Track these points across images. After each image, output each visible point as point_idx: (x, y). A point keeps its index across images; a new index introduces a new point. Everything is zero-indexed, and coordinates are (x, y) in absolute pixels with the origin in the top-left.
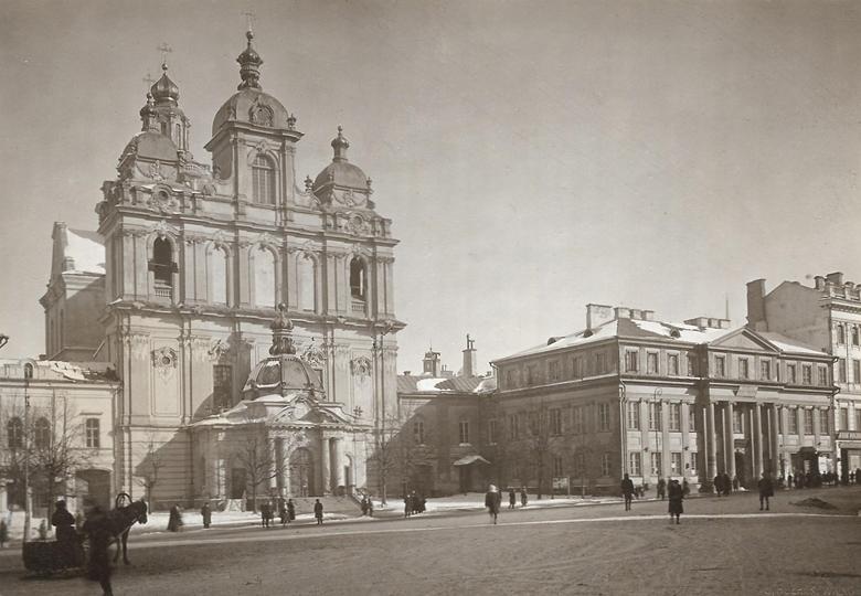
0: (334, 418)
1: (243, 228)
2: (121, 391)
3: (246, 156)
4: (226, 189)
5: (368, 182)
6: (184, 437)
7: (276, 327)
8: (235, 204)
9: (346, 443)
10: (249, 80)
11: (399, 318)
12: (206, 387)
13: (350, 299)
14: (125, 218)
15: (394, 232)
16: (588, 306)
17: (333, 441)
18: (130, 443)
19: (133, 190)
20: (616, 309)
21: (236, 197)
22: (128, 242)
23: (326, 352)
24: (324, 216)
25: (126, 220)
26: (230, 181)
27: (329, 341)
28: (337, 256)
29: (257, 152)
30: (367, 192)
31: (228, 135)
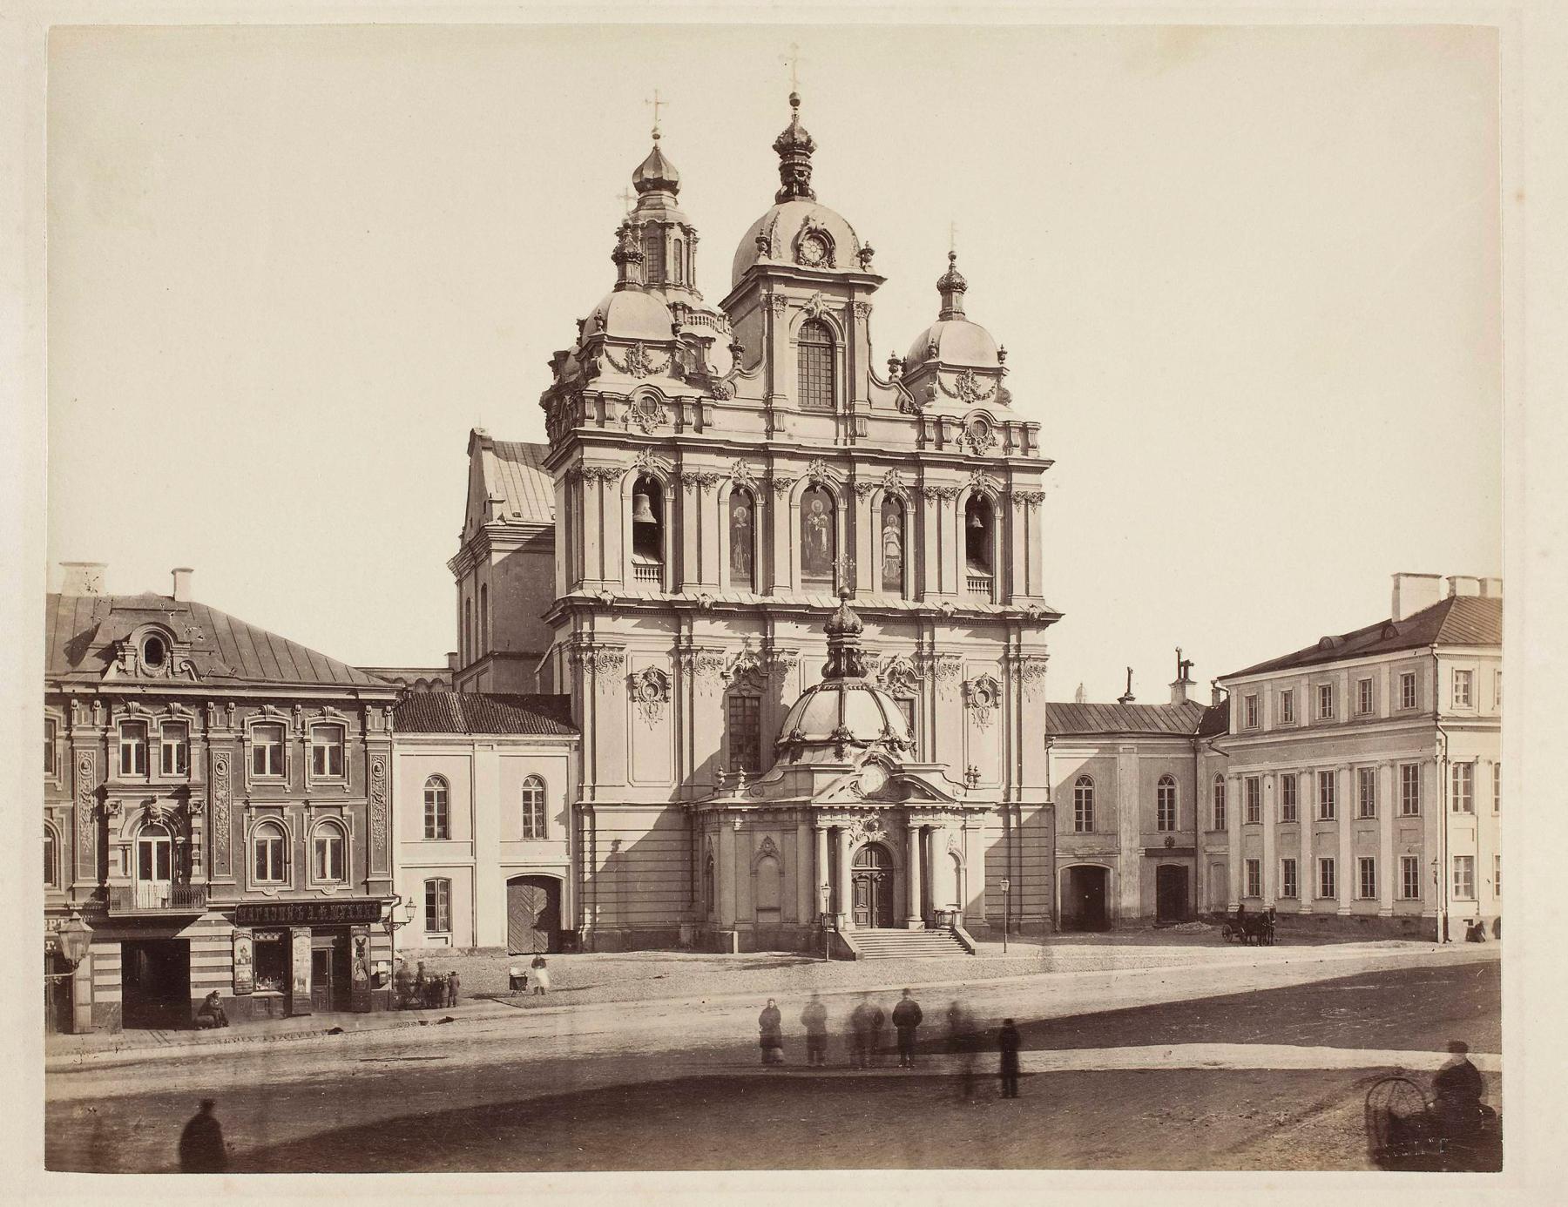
0: (929, 792)
1: (782, 455)
2: (580, 747)
3: (787, 328)
4: (752, 388)
5: (1001, 355)
6: (679, 819)
7: (836, 632)
8: (769, 413)
9: (947, 831)
10: (794, 184)
11: (1052, 604)
12: (711, 734)
13: (967, 570)
14: (586, 449)
15: (1045, 445)
16: (1397, 576)
17: (925, 831)
18: (593, 831)
19: (600, 399)
20: (1452, 580)
21: (768, 399)
22: (591, 487)
23: (921, 669)
24: (920, 423)
25: (589, 452)
26: (760, 372)
27: (926, 650)
28: (942, 496)
29: (806, 316)
30: (998, 373)
31: (755, 289)
